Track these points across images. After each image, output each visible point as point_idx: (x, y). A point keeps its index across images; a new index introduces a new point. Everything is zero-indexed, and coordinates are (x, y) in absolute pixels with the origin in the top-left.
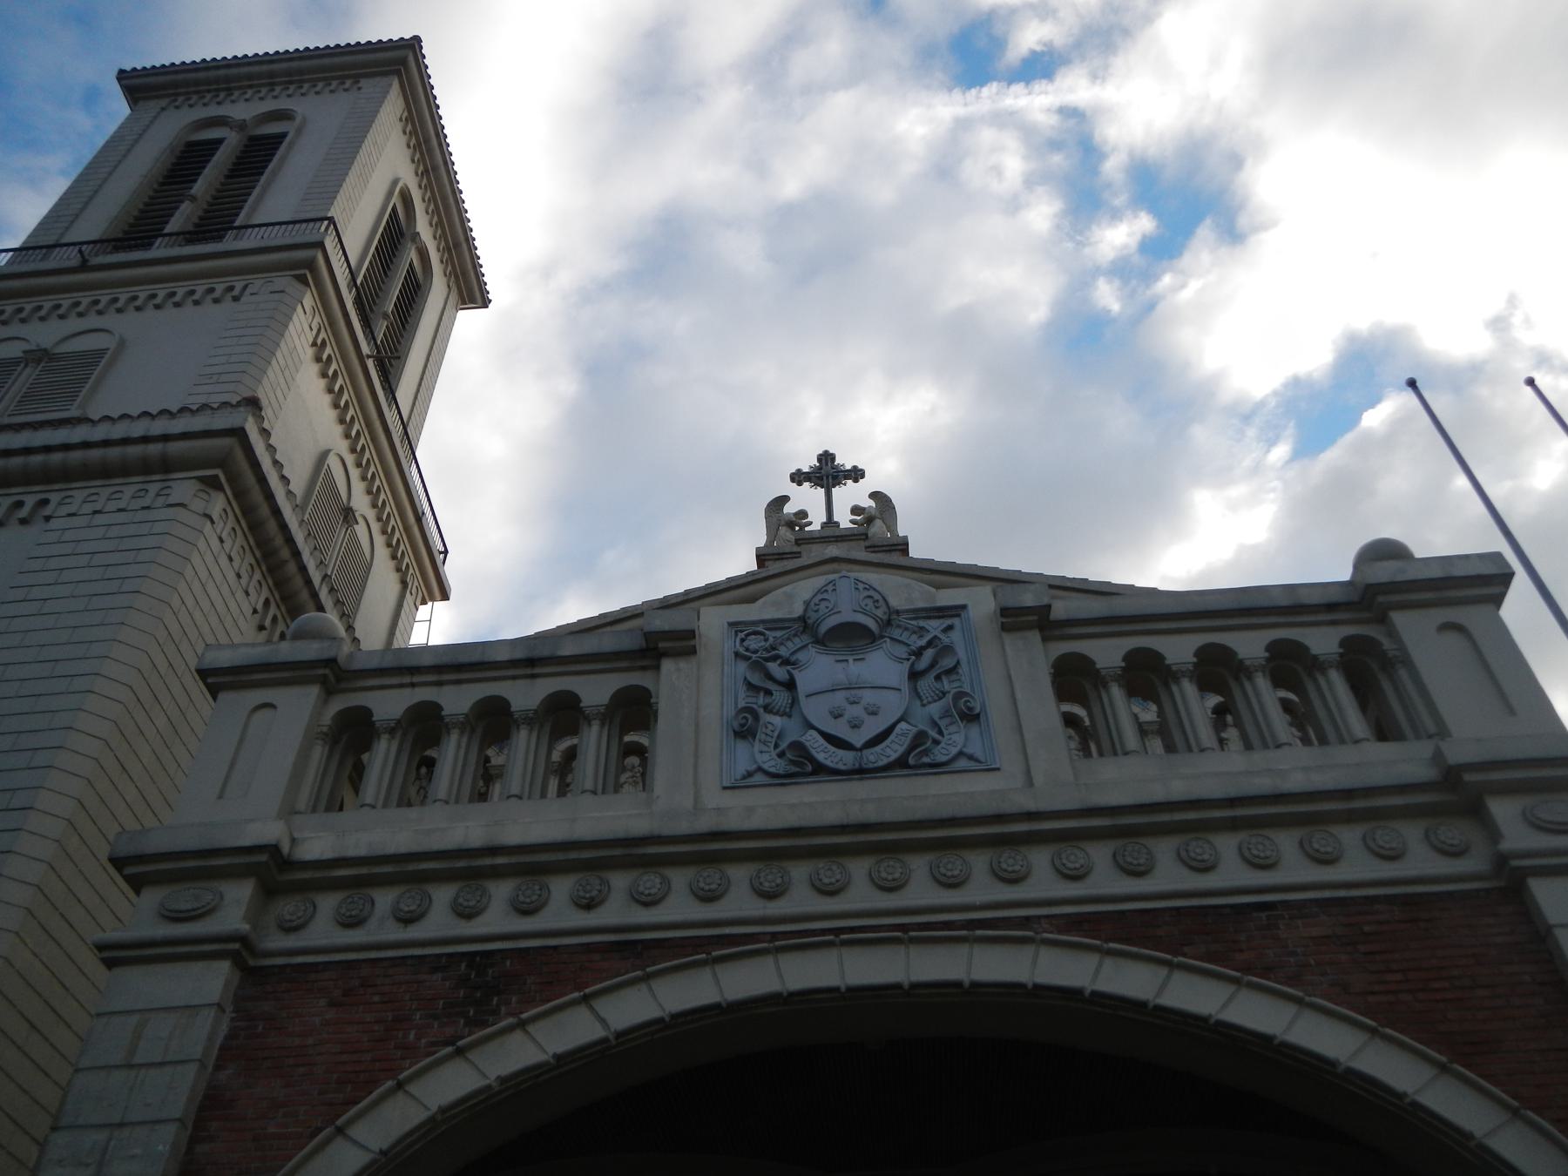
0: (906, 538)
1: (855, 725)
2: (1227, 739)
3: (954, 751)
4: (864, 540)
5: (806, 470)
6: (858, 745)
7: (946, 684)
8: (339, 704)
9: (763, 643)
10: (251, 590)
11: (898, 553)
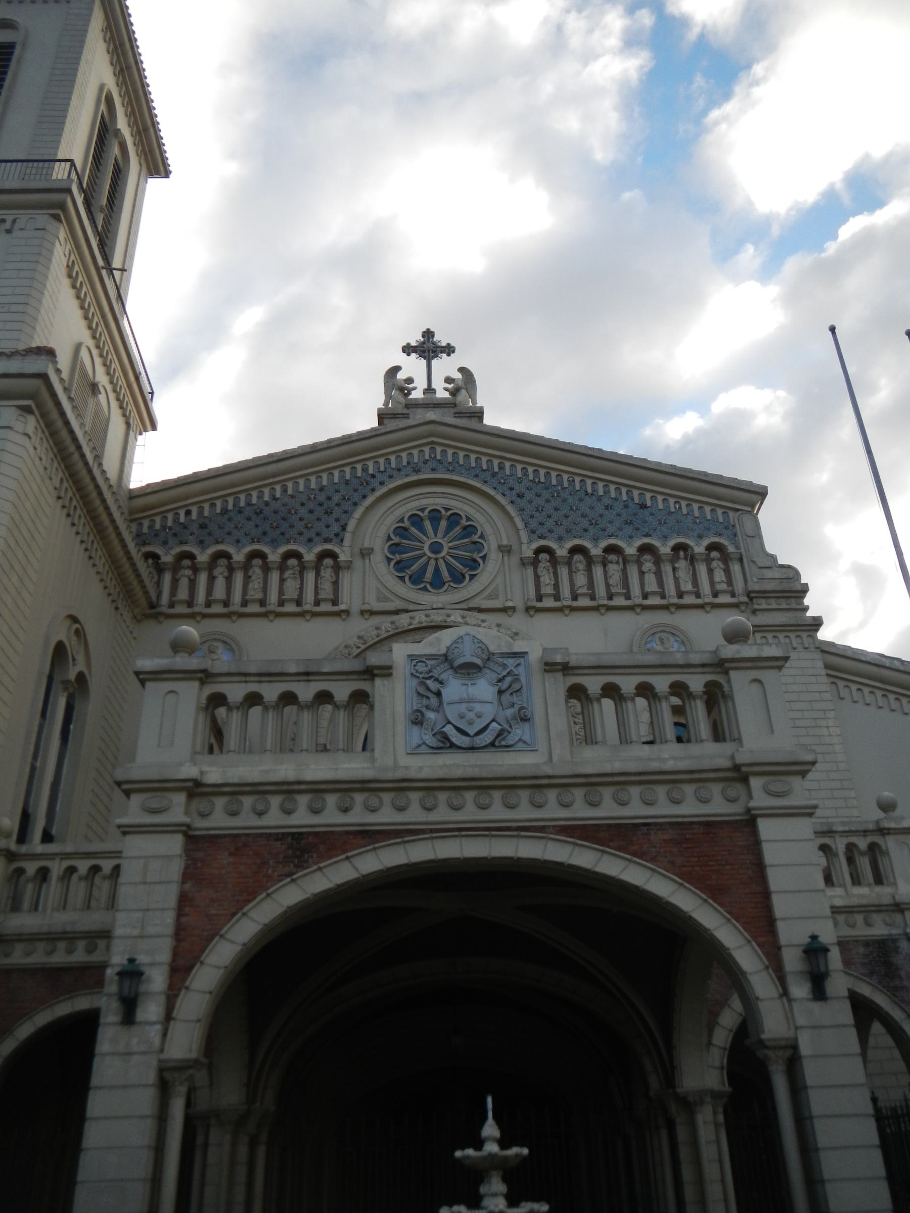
0: (482, 408)
1: (471, 723)
2: (678, 568)
3: (517, 738)
4: (453, 407)
5: (413, 344)
6: (472, 733)
7: (515, 698)
8: (209, 690)
9: (425, 669)
10: (53, 477)
11: (476, 418)
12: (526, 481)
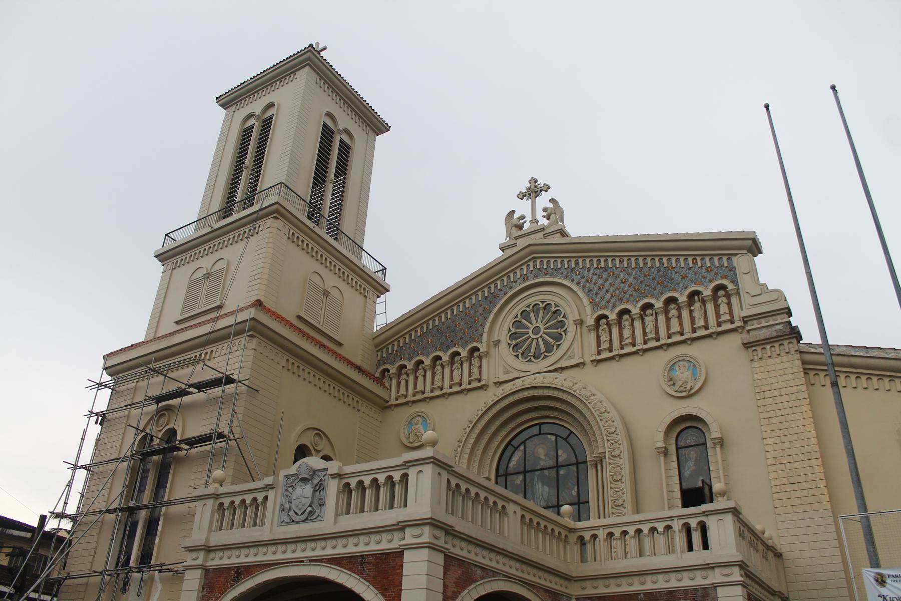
5: (524, 191)
12: (593, 269)
